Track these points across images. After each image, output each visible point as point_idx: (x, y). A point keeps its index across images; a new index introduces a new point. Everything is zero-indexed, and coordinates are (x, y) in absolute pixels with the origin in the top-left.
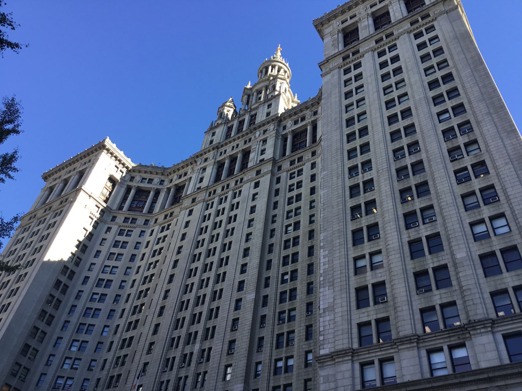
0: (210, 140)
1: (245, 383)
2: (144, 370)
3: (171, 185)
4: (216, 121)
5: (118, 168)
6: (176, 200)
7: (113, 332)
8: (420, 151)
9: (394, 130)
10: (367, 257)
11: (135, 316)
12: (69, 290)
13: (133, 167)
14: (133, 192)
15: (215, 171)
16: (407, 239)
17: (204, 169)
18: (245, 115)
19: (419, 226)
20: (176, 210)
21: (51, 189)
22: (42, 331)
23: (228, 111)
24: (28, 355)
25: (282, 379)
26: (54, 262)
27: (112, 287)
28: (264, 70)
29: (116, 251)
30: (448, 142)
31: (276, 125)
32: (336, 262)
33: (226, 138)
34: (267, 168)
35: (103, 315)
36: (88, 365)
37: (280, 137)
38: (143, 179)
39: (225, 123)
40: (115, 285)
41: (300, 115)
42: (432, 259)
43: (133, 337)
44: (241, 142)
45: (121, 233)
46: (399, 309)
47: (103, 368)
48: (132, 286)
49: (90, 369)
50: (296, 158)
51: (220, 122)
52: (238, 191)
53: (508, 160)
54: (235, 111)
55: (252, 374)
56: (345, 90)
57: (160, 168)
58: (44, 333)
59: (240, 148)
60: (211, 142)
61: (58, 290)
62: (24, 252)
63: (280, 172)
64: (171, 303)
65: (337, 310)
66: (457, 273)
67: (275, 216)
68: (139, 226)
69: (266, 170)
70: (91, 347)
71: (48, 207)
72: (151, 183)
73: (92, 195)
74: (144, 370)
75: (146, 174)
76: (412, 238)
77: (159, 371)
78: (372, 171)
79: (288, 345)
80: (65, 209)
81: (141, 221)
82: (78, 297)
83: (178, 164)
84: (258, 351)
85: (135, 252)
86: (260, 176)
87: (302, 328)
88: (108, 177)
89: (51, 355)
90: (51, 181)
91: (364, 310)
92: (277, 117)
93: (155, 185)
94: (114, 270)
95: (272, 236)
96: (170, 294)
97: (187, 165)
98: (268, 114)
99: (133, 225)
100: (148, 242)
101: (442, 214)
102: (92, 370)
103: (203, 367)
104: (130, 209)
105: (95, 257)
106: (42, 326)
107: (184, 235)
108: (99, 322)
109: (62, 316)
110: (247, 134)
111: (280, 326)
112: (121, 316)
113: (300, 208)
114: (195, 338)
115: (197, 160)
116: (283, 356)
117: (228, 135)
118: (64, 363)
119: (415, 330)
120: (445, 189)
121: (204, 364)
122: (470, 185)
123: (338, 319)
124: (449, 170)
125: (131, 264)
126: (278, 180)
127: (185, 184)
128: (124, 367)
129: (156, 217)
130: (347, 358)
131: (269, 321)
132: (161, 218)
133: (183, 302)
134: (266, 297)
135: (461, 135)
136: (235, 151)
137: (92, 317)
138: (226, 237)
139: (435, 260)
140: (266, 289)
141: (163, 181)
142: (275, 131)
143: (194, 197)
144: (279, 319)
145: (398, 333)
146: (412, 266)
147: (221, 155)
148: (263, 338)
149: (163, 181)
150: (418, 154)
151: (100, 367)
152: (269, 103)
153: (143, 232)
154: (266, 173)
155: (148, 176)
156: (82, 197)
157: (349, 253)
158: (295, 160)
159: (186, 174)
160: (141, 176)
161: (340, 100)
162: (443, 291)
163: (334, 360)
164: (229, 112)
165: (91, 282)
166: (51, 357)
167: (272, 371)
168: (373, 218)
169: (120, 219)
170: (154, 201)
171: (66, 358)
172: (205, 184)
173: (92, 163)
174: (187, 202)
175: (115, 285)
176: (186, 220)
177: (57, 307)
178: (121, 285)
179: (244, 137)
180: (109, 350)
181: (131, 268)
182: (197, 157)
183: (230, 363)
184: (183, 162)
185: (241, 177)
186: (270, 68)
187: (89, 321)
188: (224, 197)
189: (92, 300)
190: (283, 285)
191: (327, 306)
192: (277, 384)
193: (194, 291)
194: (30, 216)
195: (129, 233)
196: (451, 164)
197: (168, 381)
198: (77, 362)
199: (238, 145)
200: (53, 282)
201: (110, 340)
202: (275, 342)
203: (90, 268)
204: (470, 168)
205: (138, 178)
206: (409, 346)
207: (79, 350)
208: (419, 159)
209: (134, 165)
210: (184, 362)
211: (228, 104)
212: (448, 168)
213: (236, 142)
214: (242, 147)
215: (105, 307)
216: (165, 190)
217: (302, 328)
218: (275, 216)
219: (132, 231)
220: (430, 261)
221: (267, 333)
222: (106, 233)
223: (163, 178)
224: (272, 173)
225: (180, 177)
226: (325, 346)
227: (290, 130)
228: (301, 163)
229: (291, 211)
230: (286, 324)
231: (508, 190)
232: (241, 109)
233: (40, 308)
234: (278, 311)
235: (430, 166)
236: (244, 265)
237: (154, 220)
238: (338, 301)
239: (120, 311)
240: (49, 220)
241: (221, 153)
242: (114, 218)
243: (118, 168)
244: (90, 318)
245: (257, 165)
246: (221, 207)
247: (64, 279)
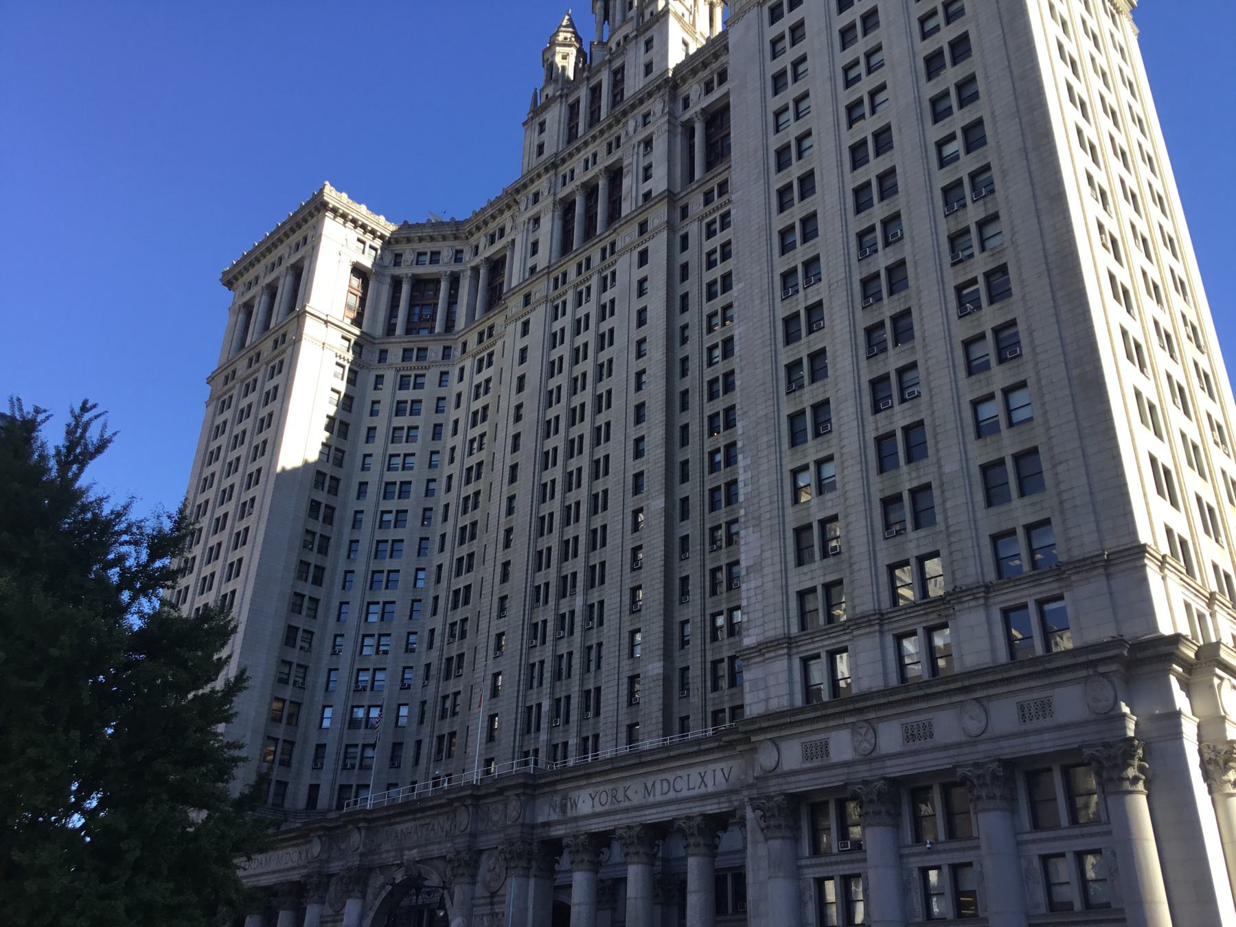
0: (536, 143)
1: (664, 660)
2: (499, 647)
4: (542, 90)
5: (364, 243)
6: (494, 297)
7: (433, 578)
8: (902, 238)
9: (860, 182)
10: (812, 467)
11: (465, 546)
12: (337, 513)
13: (393, 233)
14: (405, 289)
15: (558, 223)
16: (874, 435)
17: (536, 220)
18: (599, 71)
19: (892, 407)
20: (498, 321)
21: (248, 308)
22: (311, 598)
23: (564, 57)
24: (299, 643)
25: (725, 648)
26: (295, 470)
27: (412, 494)
29: (404, 421)
30: (950, 218)
31: (667, 99)
32: (764, 480)
33: (569, 142)
34: (658, 215)
35: (409, 548)
36: (404, 643)
37: (679, 129)
38: (420, 254)
39: (561, 96)
40: (417, 489)
41: (715, 66)
42: (909, 473)
43: (470, 586)
44: (599, 147)
45: (403, 385)
46: (856, 567)
47: (430, 646)
48: (449, 489)
49: (409, 649)
50: (714, 184)
51: (550, 91)
52: (608, 272)
53: (1044, 267)
54: (580, 52)
55: (677, 642)
56: (774, 67)
57: (448, 224)
58: (315, 601)
59: (601, 166)
60: (541, 148)
61: (317, 519)
62: (235, 454)
63: (686, 221)
64: (522, 520)
65: (766, 571)
66: (944, 502)
67: (685, 327)
69: (656, 222)
70: (401, 609)
71: (252, 353)
72: (437, 262)
73: (330, 319)
74: (499, 647)
75: (424, 243)
76: (881, 432)
78: (822, 284)
79: (729, 588)
80: (286, 357)
81: (435, 351)
82: (356, 523)
83: (483, 210)
84: (681, 603)
85: (439, 418)
86: (646, 236)
88: (349, 269)
89: (336, 636)
90: (242, 289)
91: (805, 568)
92: (667, 80)
93: (445, 267)
94: (409, 460)
95: (684, 373)
96: (516, 503)
97: (501, 212)
98: (648, 68)
99: (424, 364)
100: (459, 395)
101: (929, 384)
102: (413, 651)
103: (595, 636)
104: (408, 331)
105: (367, 442)
106: (307, 589)
107: (521, 379)
108: (405, 563)
109: (336, 562)
110: (610, 127)
111: (714, 554)
112: (442, 549)
113: (730, 306)
114: (574, 586)
115: (517, 198)
116: (724, 607)
117: (572, 135)
119: (879, 602)
120: (937, 329)
121: (595, 630)
122: (978, 319)
123: (768, 586)
124: (947, 287)
125: (436, 446)
126: (685, 238)
127: (505, 256)
128: (465, 640)
129: (462, 340)
130: (781, 652)
131: (694, 547)
132: (472, 339)
133: (543, 518)
134: (685, 501)
135: (974, 202)
136: (591, 174)
137: (391, 557)
138: (601, 380)
139: (914, 474)
140: (684, 485)
141: (462, 251)
142: (666, 118)
143: (526, 291)
144: (713, 541)
145: (854, 608)
146: (879, 487)
147: (564, 184)
148: (687, 577)
150: (898, 244)
151: (425, 645)
152: (648, 35)
154: (657, 231)
155: (428, 247)
156: (311, 327)
157: (784, 462)
158: (712, 190)
159: (502, 231)
160: (413, 250)
161: (764, 99)
162: (921, 532)
163: (763, 655)
164: (566, 60)
165: (372, 491)
166: (338, 639)
167: (708, 635)
168: (821, 390)
169: (395, 355)
170: (452, 300)
171: (364, 636)
172: (542, 259)
173: (310, 244)
174: (514, 304)
175: (417, 489)
176: (517, 344)
177: (323, 550)
178: (427, 489)
179: (606, 135)
180: (434, 613)
181: (438, 452)
182: (517, 191)
183: (637, 626)
184: (491, 204)
185: (610, 239)
187: (388, 564)
188: (583, 287)
189: (383, 524)
190: (714, 475)
191: (751, 563)
192: (718, 657)
193: (558, 495)
194: (225, 373)
195: (419, 380)
196: (951, 270)
197: (542, 662)
198: (384, 640)
199: (595, 155)
200: (305, 506)
201: (432, 594)
202: (708, 584)
204: (981, 279)
205: (409, 257)
206: (867, 630)
207: (382, 619)
208: (899, 257)
209: (392, 227)
210: (563, 629)
211: (561, 37)
212: (946, 280)
213: (591, 149)
214: (605, 161)
215: (409, 533)
216: (469, 272)
218: (685, 327)
219: (424, 375)
220: (906, 477)
221: (692, 568)
222: (376, 388)
223: (458, 245)
224: (671, 226)
225: (492, 242)
226: (751, 632)
227: (698, 108)
228: (725, 198)
229: (715, 314)
230: (724, 550)
231: (1035, 334)
232: (592, 43)
233: (294, 560)
234: (708, 526)
235: (917, 278)
236: (639, 441)
238: (767, 554)
239: (438, 539)
240: (263, 383)
241: (564, 177)
242: (383, 353)
243: (364, 243)
244: (388, 560)
245: (640, 210)
246: (580, 313)
247: (322, 497)
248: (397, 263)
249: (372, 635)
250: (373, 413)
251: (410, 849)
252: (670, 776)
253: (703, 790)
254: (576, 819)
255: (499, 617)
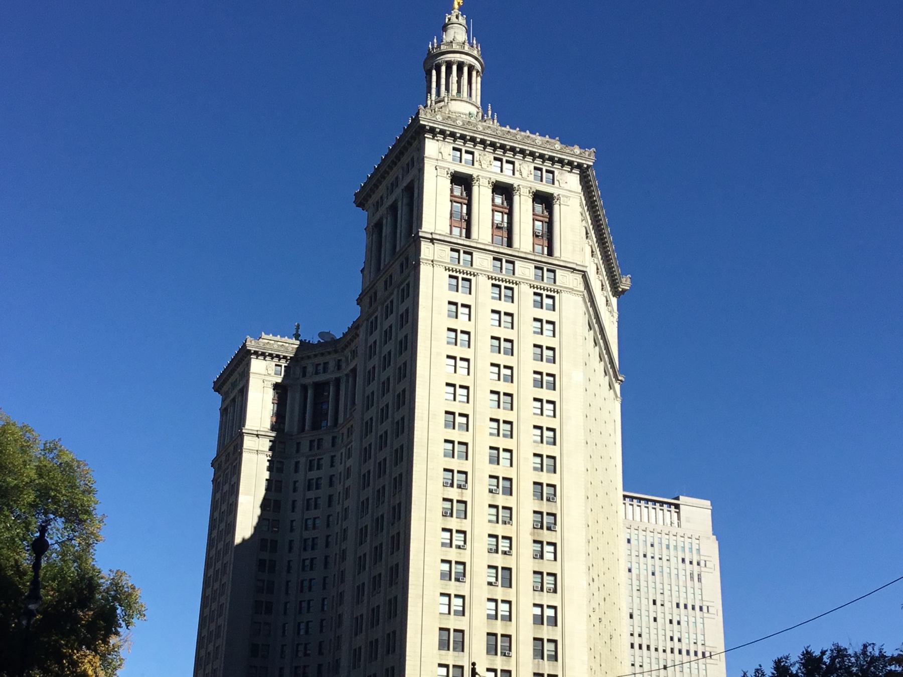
14: (310, 393)
38: (318, 365)
40: (321, 543)
81: (327, 443)
118: (297, 651)
149: (340, 361)
153: (333, 457)
155: (320, 360)
169: (305, 447)
175: (321, 543)
203: (292, 526)
242: (298, 444)
248: (304, 375)
250: (295, 490)
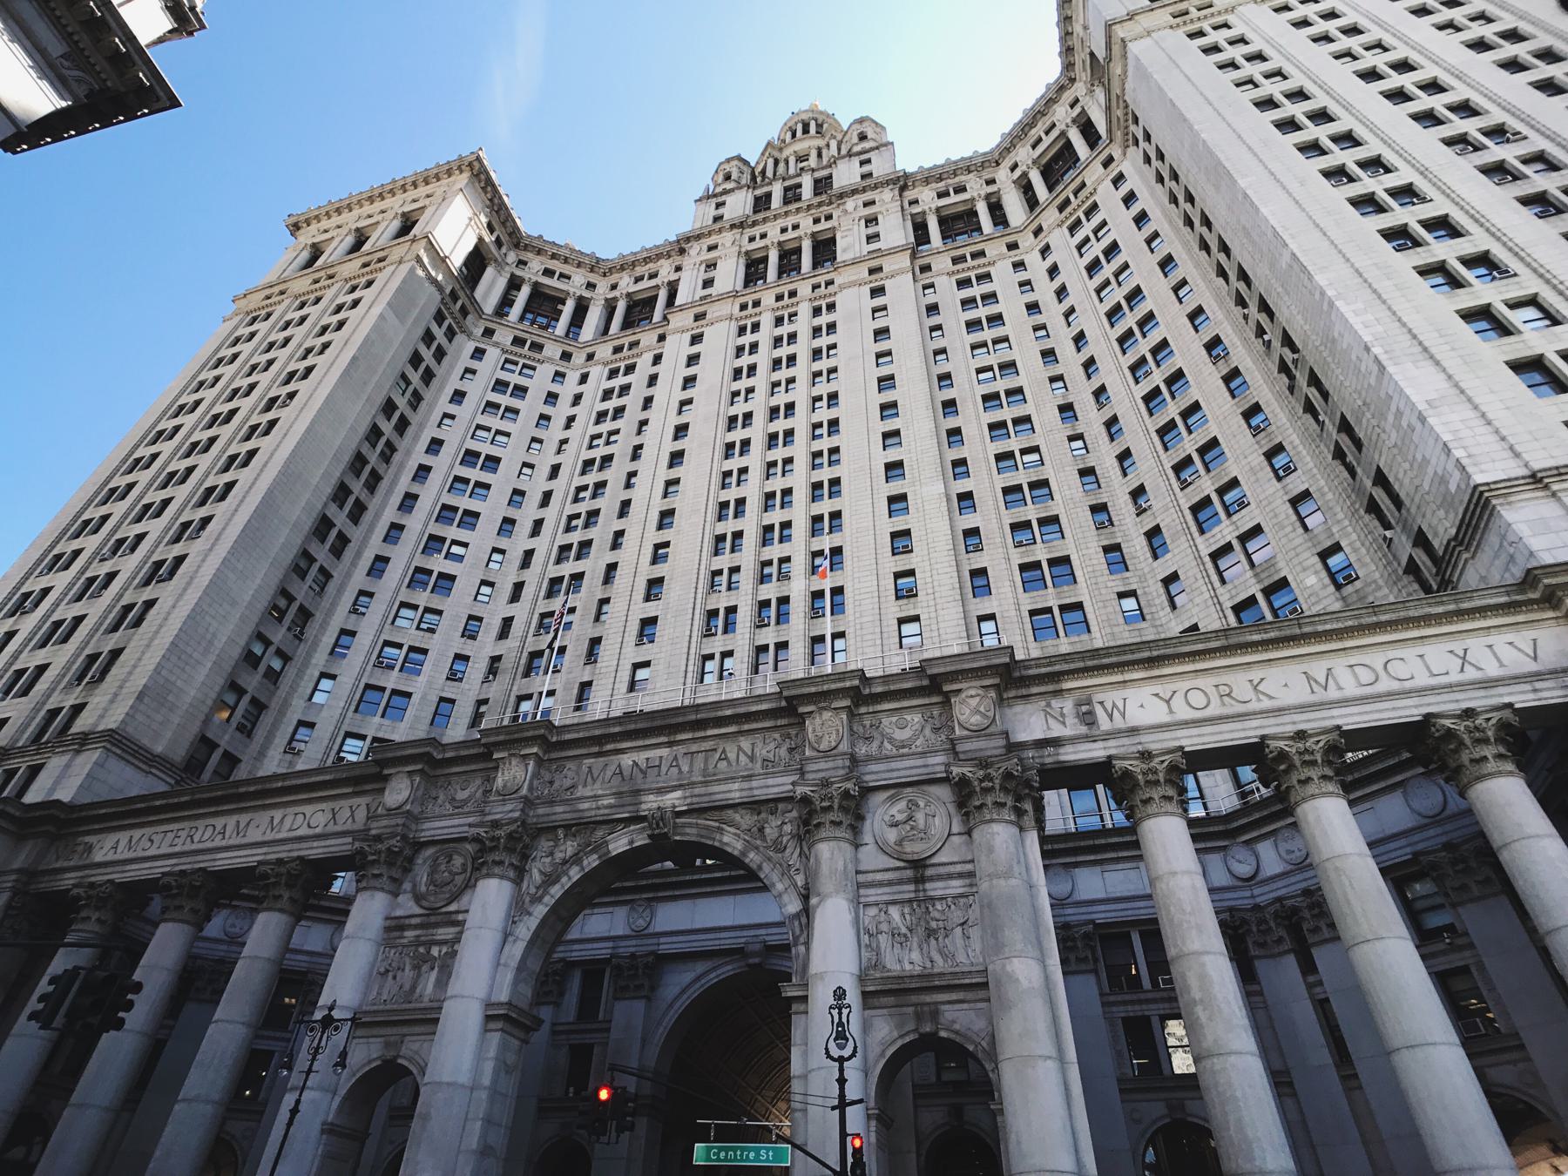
0: (712, 212)
3: (616, 293)
7: (517, 563)
14: (525, 291)
20: (648, 338)
28: (799, 128)
68: (550, 360)
77: (695, 634)
87: (1092, 551)
99: (537, 356)
102: (473, 638)
129: (590, 350)
132: (604, 351)
169: (504, 336)
175: (509, 467)
183: (912, 613)
186: (813, 124)
194: (267, 292)
200: (363, 428)
201: (513, 578)
217: (1092, 551)
223: (593, 278)
225: (638, 280)
237: (584, 356)
242: (489, 333)
249: (415, 607)
251: (661, 791)
252: (1376, 659)
253: (1471, 674)
254: (1134, 731)
255: (647, 599)
